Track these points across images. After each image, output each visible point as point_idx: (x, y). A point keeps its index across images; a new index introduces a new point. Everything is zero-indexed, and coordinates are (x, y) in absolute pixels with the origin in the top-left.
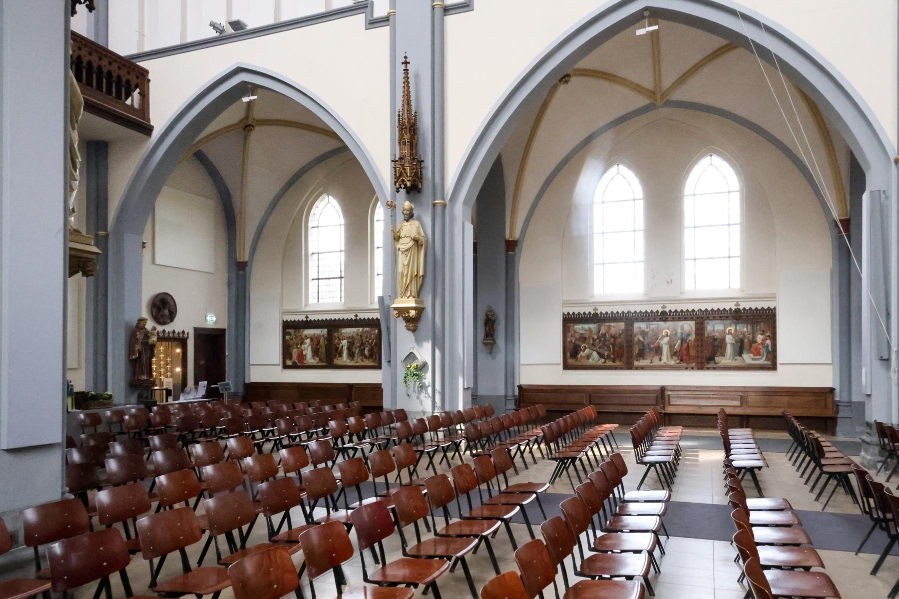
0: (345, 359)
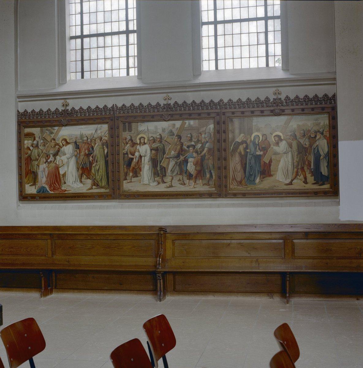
0: (146, 181)
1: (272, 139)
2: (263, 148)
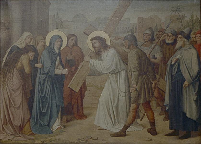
1: (88, 45)
2: (68, 61)
